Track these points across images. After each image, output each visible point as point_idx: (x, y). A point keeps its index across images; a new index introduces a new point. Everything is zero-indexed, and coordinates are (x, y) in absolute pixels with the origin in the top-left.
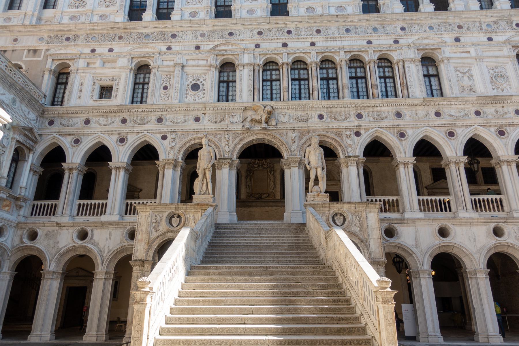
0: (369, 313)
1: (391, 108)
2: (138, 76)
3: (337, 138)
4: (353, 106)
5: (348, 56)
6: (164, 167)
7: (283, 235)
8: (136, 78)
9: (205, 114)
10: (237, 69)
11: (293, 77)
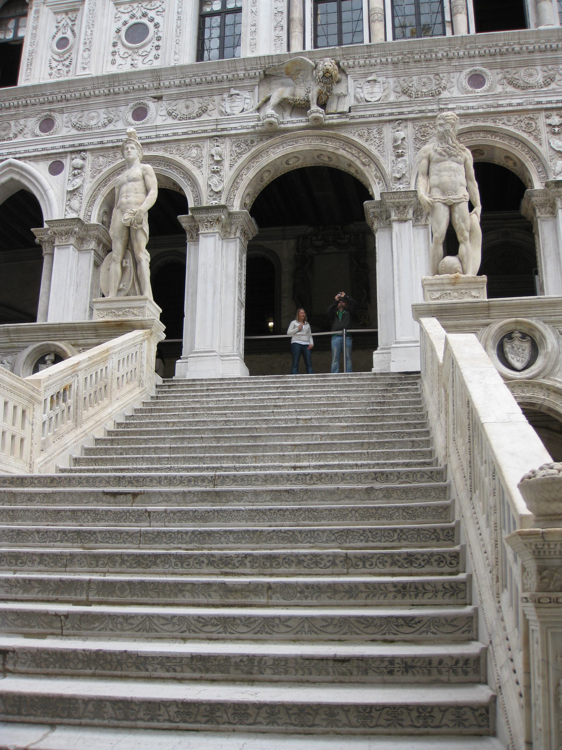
3: (525, 136)
7: (345, 400)
9: (159, 98)
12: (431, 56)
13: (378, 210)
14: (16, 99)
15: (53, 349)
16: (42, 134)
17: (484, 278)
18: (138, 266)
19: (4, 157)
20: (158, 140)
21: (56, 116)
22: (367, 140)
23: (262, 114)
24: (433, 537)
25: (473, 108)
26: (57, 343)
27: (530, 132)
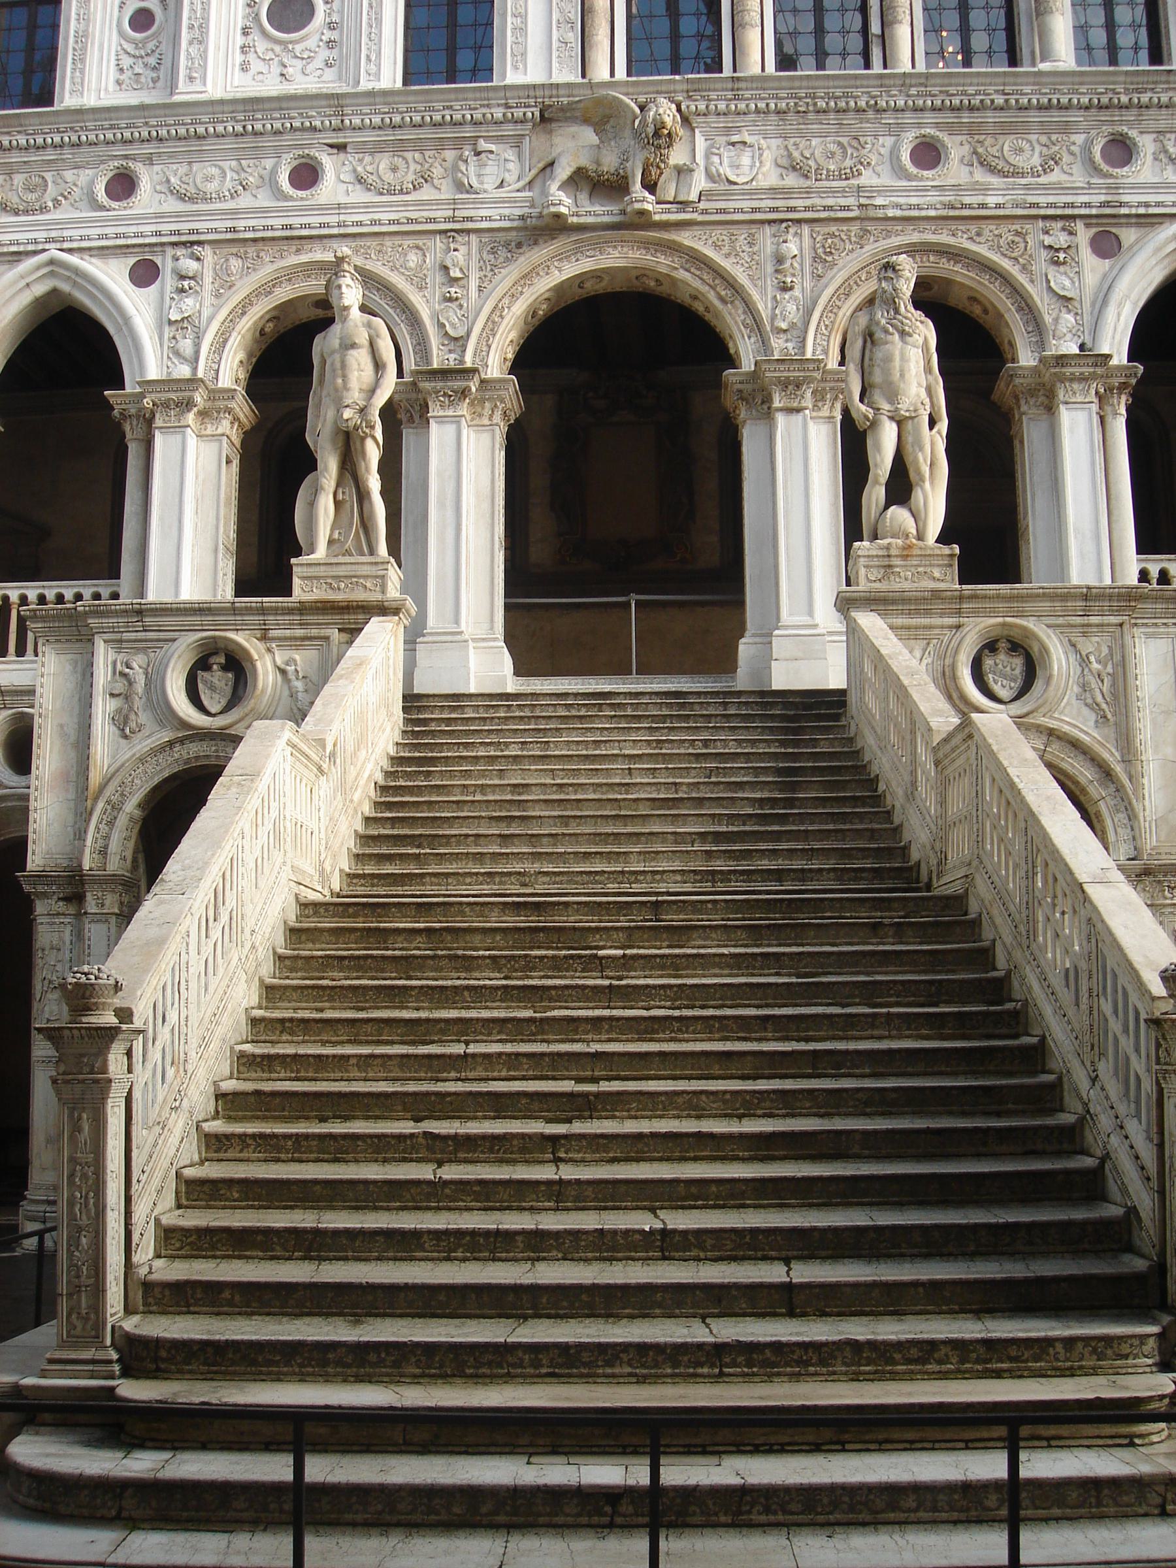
0: (1122, 1109)
3: (1006, 264)
4: (1085, 100)
6: (149, 422)
9: (341, 147)
12: (847, 103)
15: (221, 645)
16: (115, 204)
19: (40, 247)
20: (342, 231)
21: (139, 168)
22: (727, 256)
25: (918, 207)
26: (231, 635)
27: (1016, 259)
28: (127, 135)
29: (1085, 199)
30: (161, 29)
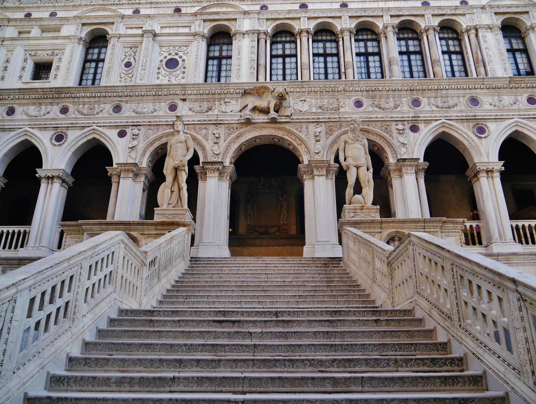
1: (462, 92)
2: (91, 51)
4: (406, 88)
5: (397, 21)
6: (119, 176)
7: (304, 272)
8: (87, 54)
9: (184, 100)
10: (234, 38)
11: (316, 51)
13: (306, 170)
14: (99, 92)
17: (378, 207)
18: (181, 191)
22: (300, 132)
23: (242, 113)
24: (435, 349)
28: (120, 94)
29: (408, 115)
30: (134, 67)
